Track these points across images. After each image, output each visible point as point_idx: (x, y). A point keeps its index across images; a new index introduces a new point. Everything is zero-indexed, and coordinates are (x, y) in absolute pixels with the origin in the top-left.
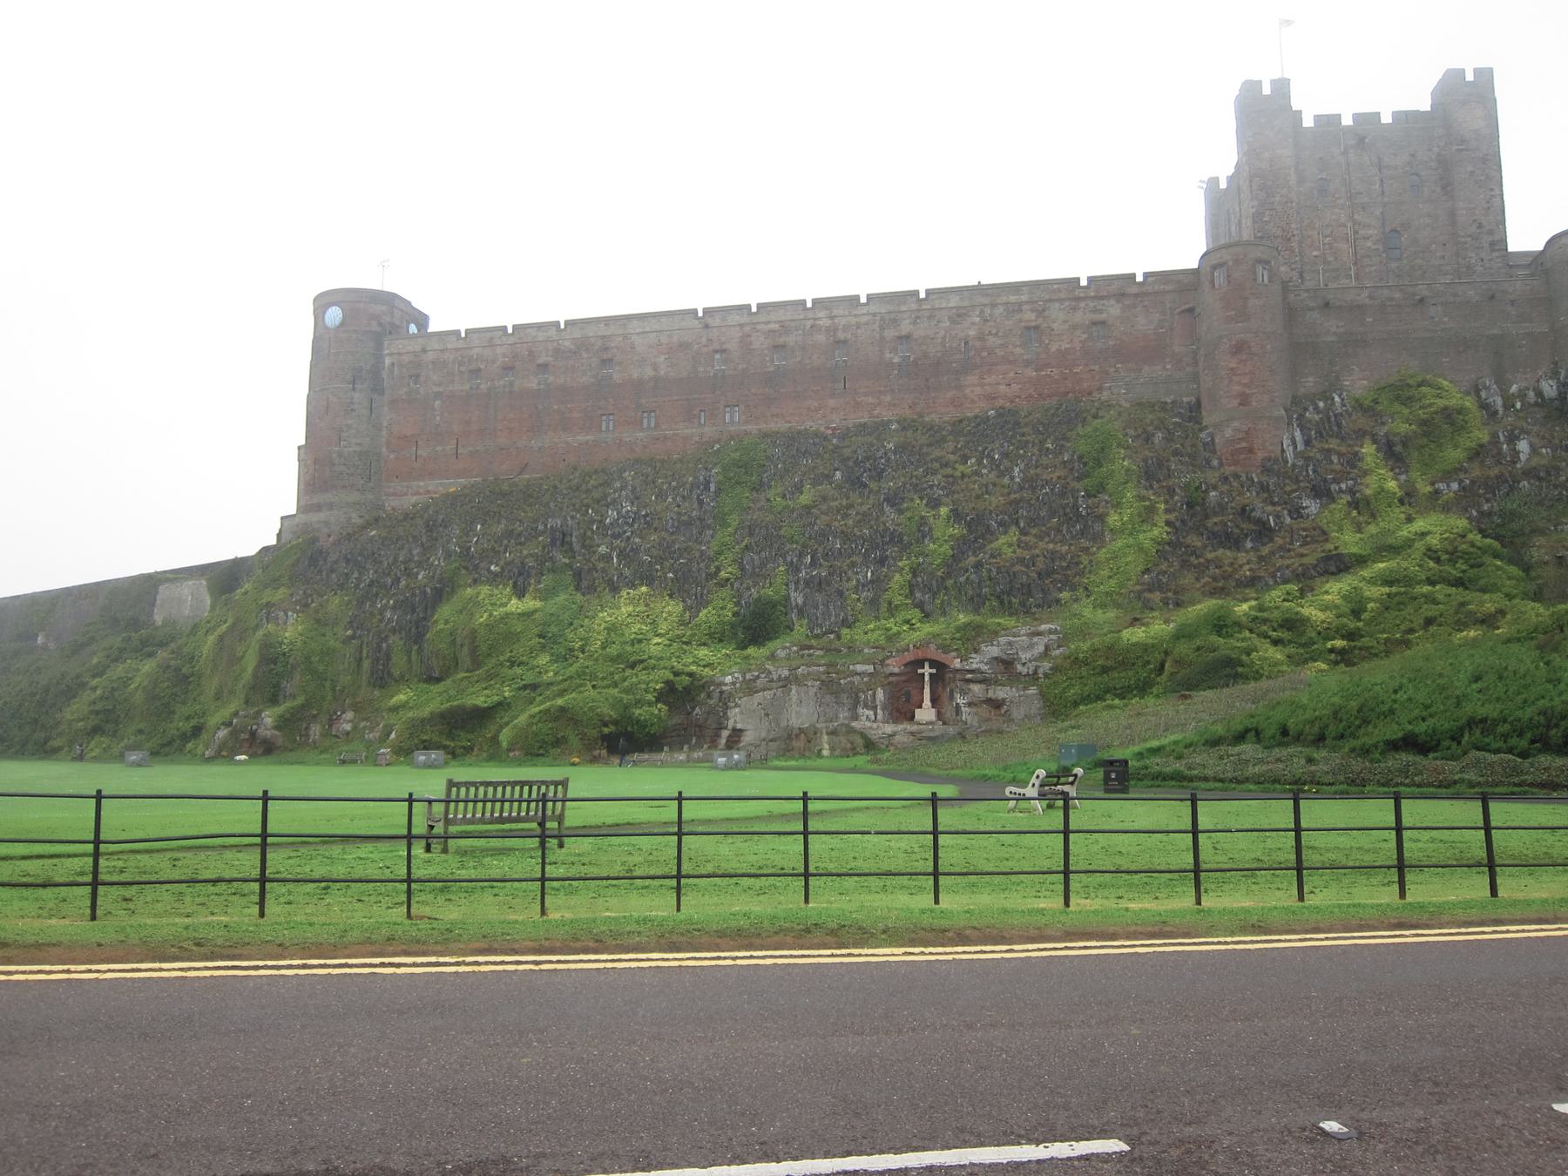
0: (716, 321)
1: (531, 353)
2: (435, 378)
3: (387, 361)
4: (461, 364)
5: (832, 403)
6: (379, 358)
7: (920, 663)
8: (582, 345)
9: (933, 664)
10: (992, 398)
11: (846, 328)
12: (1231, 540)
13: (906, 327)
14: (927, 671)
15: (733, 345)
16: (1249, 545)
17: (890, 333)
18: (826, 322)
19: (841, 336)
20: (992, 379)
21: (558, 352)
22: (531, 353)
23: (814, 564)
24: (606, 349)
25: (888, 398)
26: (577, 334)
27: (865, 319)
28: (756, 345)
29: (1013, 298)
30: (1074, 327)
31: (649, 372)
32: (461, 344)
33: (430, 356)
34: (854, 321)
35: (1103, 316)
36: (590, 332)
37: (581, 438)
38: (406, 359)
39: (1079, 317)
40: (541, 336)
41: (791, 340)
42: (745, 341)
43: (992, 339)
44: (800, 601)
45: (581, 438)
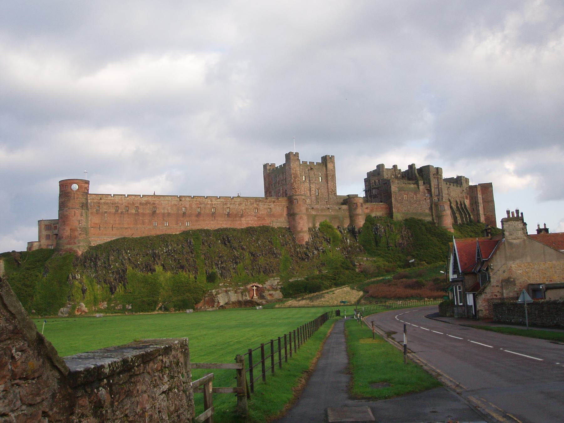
0: (183, 199)
1: (133, 203)
3: (89, 201)
5: (212, 222)
7: (253, 286)
8: (147, 203)
9: (256, 286)
10: (248, 224)
11: (215, 204)
12: (303, 259)
13: (228, 205)
14: (255, 288)
15: (188, 206)
16: (306, 260)
18: (210, 202)
19: (214, 206)
20: (248, 219)
21: (141, 204)
22: (133, 203)
23: (222, 263)
24: (154, 204)
25: (225, 222)
26: (146, 199)
31: (166, 211)
33: (103, 201)
36: (150, 199)
39: (266, 207)
41: (202, 206)
42: (191, 206)
43: (247, 210)
44: (220, 272)
45: (149, 227)
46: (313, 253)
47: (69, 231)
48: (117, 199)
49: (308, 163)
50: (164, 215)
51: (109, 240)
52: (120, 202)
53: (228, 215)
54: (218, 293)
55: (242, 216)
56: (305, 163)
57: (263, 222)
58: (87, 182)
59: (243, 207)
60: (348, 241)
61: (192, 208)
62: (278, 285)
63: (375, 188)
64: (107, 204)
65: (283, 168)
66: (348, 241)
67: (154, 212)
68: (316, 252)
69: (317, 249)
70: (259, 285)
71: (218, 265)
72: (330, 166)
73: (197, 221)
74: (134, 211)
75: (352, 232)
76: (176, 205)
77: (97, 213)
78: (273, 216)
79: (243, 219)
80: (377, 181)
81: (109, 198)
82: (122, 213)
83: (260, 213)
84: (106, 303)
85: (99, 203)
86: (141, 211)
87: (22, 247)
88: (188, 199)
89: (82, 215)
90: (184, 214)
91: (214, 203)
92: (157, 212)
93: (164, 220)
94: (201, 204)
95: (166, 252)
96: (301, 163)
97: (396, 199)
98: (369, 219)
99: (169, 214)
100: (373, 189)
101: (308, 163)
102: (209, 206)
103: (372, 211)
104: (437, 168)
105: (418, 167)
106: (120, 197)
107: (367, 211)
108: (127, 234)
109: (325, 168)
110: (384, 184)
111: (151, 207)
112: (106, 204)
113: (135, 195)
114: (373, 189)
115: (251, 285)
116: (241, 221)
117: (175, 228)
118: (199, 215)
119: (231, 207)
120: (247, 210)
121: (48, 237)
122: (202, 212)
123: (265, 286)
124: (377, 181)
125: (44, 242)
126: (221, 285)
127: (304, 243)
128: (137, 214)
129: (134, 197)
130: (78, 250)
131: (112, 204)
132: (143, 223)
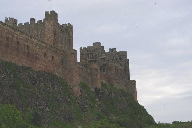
5: (16, 57)
13: (29, 44)
17: (26, 44)
19: (19, 40)
27: (22, 38)
29: (44, 45)
30: (50, 56)
34: (21, 37)
35: (53, 55)
41: (10, 36)
55: (37, 59)
59: (37, 49)
63: (93, 61)
72: (71, 33)
75: (97, 92)
79: (37, 62)
80: (94, 55)
91: (19, 37)
100: (91, 61)
110: (102, 59)
118: (7, 46)
124: (94, 55)
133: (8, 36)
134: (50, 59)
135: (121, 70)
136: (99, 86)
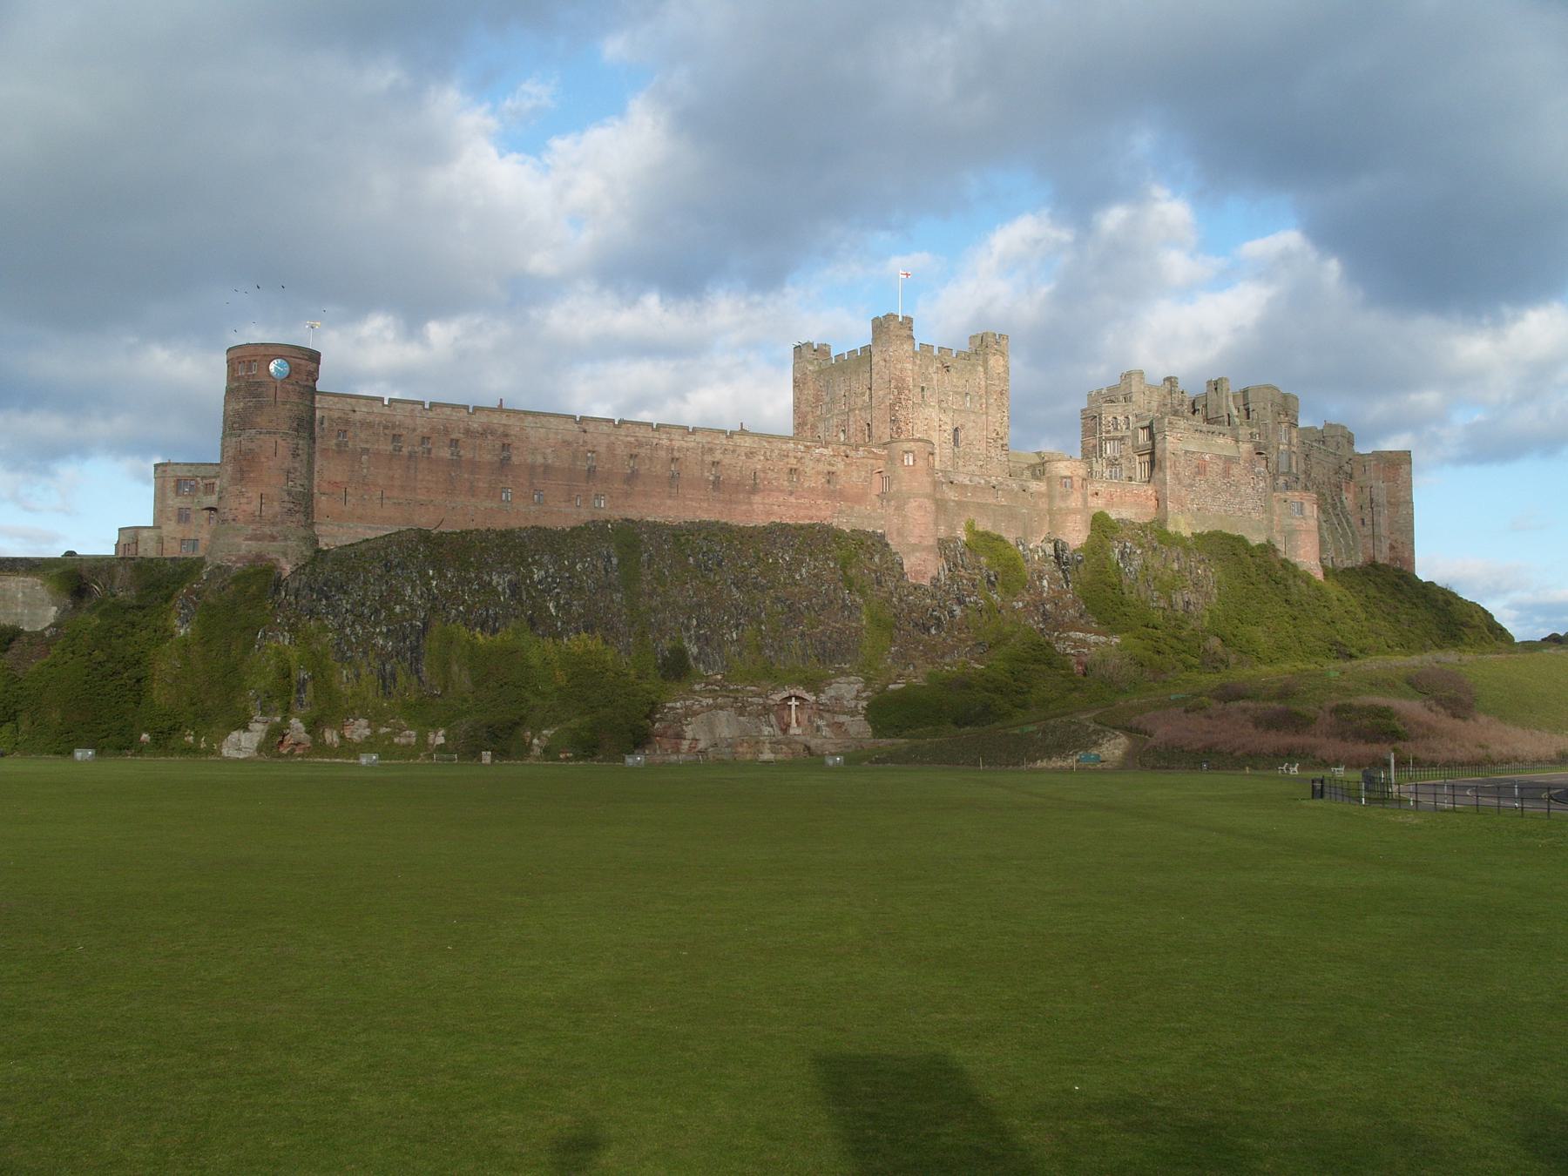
0: (591, 427)
2: (362, 436)
3: (318, 414)
4: (386, 427)
5: (669, 502)
6: (314, 409)
7: (789, 698)
8: (486, 432)
9: (797, 698)
10: (769, 514)
11: (679, 450)
13: (718, 456)
14: (793, 702)
15: (602, 449)
17: (708, 458)
19: (676, 454)
21: (468, 432)
25: (705, 505)
26: (483, 418)
28: (619, 451)
30: (818, 473)
31: (540, 460)
32: (386, 411)
33: (357, 417)
37: (488, 504)
38: (336, 415)
40: (455, 415)
41: (643, 452)
42: (611, 448)
45: (488, 504)
46: (951, 612)
47: (256, 503)
48: (399, 415)
49: (936, 352)
50: (532, 468)
51: (371, 535)
52: (408, 421)
53: (717, 484)
54: (690, 713)
55: (754, 490)
56: (927, 348)
57: (813, 512)
58: (315, 357)
60: (1045, 583)
61: (614, 456)
62: (857, 698)
64: (370, 425)
65: (864, 358)
66: (1045, 583)
67: (504, 464)
68: (958, 610)
69: (960, 602)
70: (807, 696)
71: (688, 629)
73: (627, 495)
74: (446, 453)
75: (1059, 555)
76: (567, 443)
77: (339, 452)
78: (841, 495)
79: (757, 499)
80: (1121, 419)
81: (377, 408)
82: (411, 456)
83: (806, 485)
84: (363, 722)
85: (347, 422)
86: (466, 454)
87: (98, 543)
88: (605, 428)
89: (295, 455)
90: (591, 472)
91: (677, 444)
92: (515, 460)
93: (532, 484)
94: (640, 445)
95: (540, 582)
96: (917, 348)
97: (1177, 475)
98: (1101, 526)
99: (547, 469)
100: (1107, 439)
101: (936, 352)
102: (663, 454)
103: (1110, 503)
104: (1285, 397)
105: (1235, 386)
106: (410, 406)
107: (1097, 504)
108: (424, 520)
109: (981, 369)
111: (498, 444)
112: (366, 425)
113: (453, 407)
114: (1107, 439)
115: (786, 694)
116: (751, 504)
117: (564, 514)
119: (727, 460)
120: (771, 475)
121: (183, 516)
122: (643, 469)
123: (823, 698)
124: (1121, 419)
125: (171, 528)
126: (697, 687)
127: (926, 582)
128: (456, 462)
129: (448, 411)
130: (283, 561)
131: (386, 427)
132: (472, 491)
133: (635, 451)
134: (814, 481)
135: (1229, 461)
136: (1076, 536)
